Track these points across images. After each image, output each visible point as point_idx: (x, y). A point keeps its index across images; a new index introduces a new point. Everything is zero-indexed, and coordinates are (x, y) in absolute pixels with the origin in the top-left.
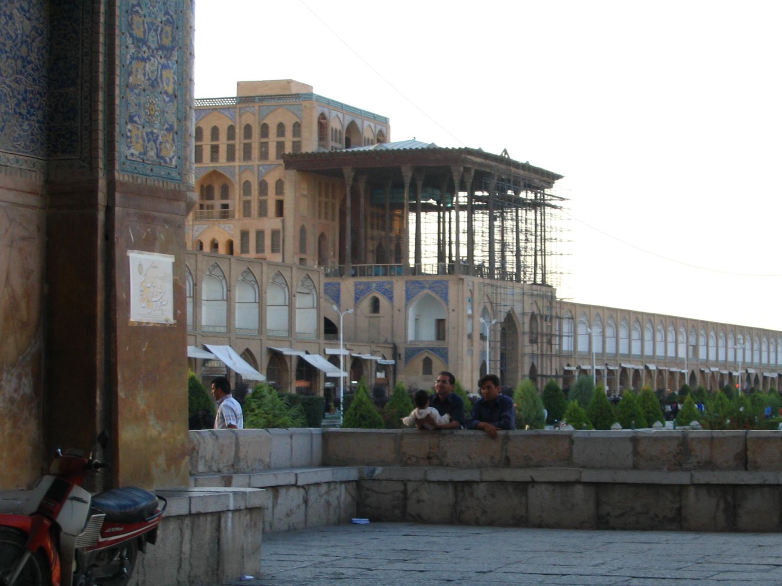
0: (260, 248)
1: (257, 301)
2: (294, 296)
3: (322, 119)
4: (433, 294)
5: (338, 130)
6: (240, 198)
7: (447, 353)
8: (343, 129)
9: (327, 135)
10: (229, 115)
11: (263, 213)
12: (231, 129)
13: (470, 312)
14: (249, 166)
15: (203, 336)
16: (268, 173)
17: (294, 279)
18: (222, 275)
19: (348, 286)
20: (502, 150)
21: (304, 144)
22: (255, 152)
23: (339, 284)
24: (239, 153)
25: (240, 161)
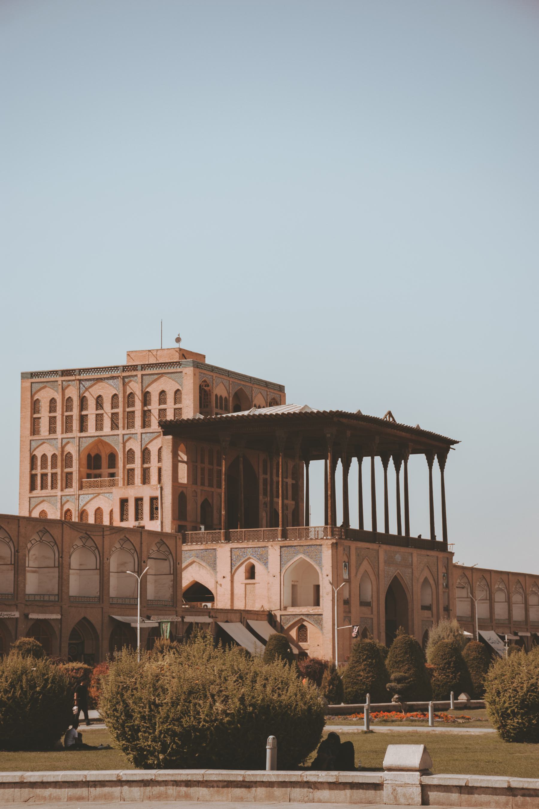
0: (138, 516)
1: (98, 568)
2: (144, 562)
3: (205, 386)
5: (224, 397)
6: (124, 467)
8: (229, 397)
9: (210, 402)
10: (113, 384)
11: (145, 480)
13: (346, 576)
15: (26, 605)
17: (144, 545)
18: (53, 541)
19: (224, 551)
20: (386, 413)
21: (184, 411)
25: (124, 429)
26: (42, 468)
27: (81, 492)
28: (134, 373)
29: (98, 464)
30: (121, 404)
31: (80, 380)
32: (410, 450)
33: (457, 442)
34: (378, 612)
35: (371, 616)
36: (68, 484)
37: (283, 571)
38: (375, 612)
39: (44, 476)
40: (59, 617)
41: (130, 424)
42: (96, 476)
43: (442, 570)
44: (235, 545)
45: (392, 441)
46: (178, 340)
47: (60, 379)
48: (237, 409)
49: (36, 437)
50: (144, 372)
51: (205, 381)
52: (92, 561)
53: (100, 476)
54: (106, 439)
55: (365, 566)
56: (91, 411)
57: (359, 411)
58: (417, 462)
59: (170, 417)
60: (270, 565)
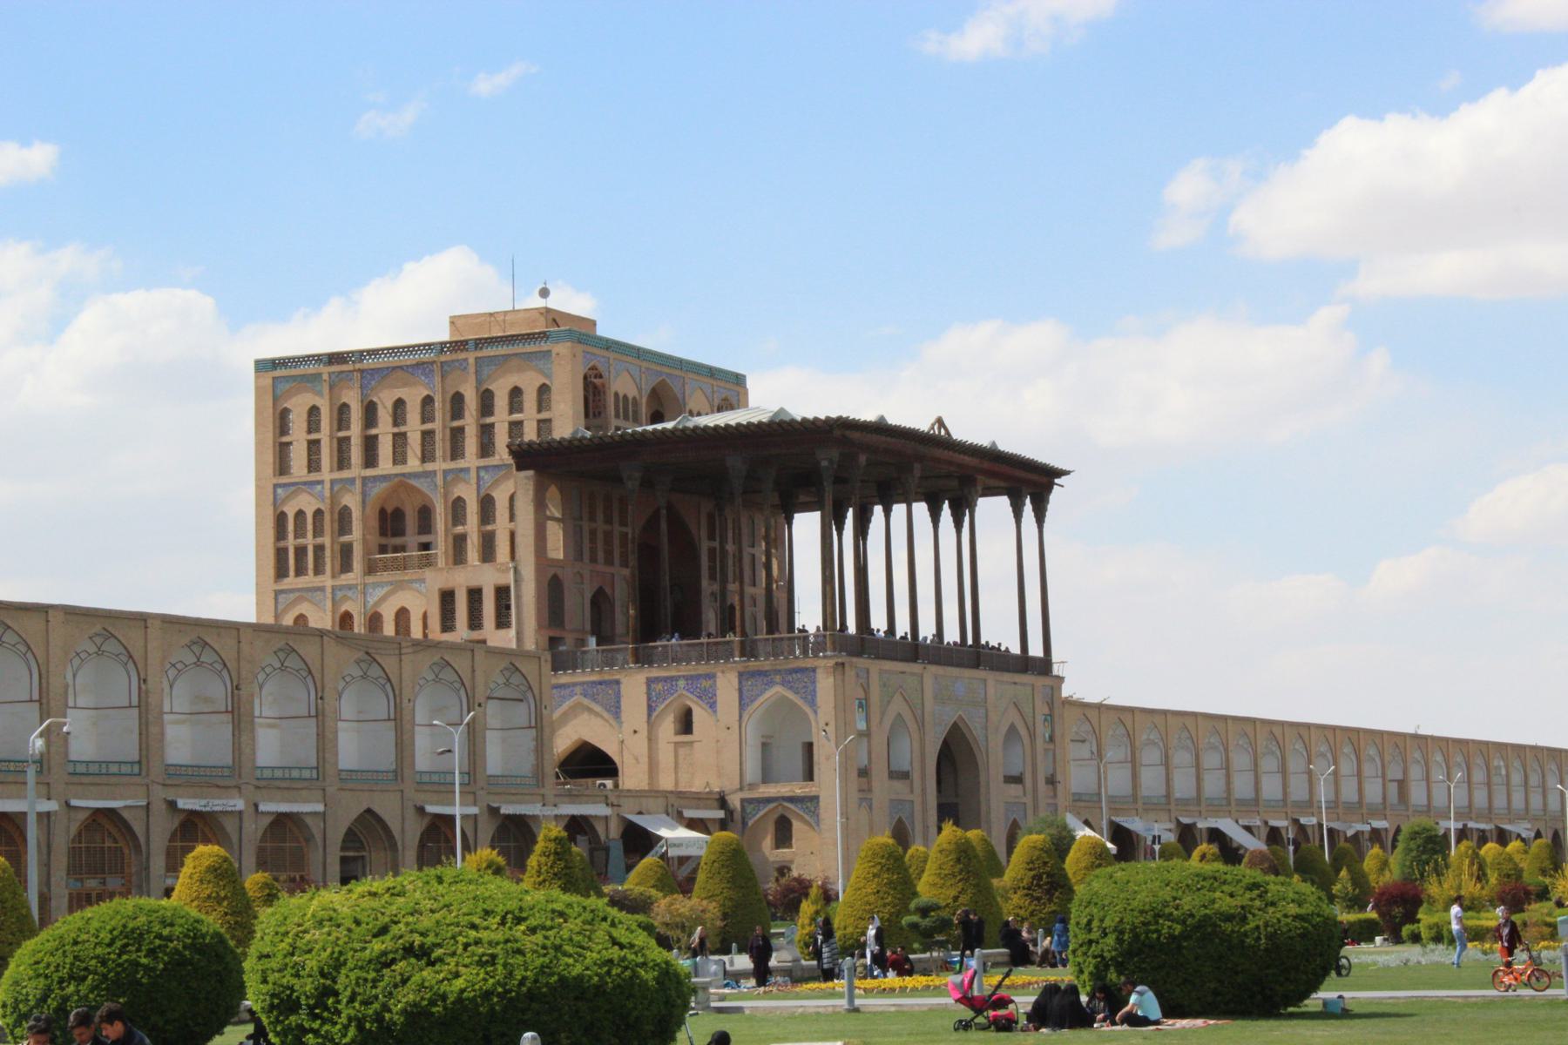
0: (475, 621)
4: (790, 695)
6: (446, 530)
7: (817, 807)
11: (488, 553)
12: (428, 401)
13: (862, 726)
14: (462, 470)
15: (257, 787)
16: (496, 483)
17: (479, 673)
19: (634, 684)
20: (933, 420)
22: (471, 443)
23: (618, 682)
24: (441, 445)
26: (296, 537)
27: (370, 579)
28: (462, 356)
29: (398, 526)
30: (438, 415)
31: (362, 371)
32: (979, 488)
33: (1066, 473)
34: (924, 790)
35: (910, 797)
36: (346, 566)
37: (745, 717)
38: (917, 789)
39: (301, 551)
40: (320, 808)
41: (456, 451)
42: (396, 549)
43: (1042, 709)
44: (655, 672)
45: (948, 473)
46: (544, 293)
47: (325, 370)
48: (657, 417)
49: (284, 480)
50: (480, 354)
51: (593, 368)
52: (380, 706)
53: (403, 548)
54: (413, 482)
55: (898, 706)
56: (384, 429)
57: (882, 418)
58: (992, 510)
59: (530, 434)
60: (719, 706)
